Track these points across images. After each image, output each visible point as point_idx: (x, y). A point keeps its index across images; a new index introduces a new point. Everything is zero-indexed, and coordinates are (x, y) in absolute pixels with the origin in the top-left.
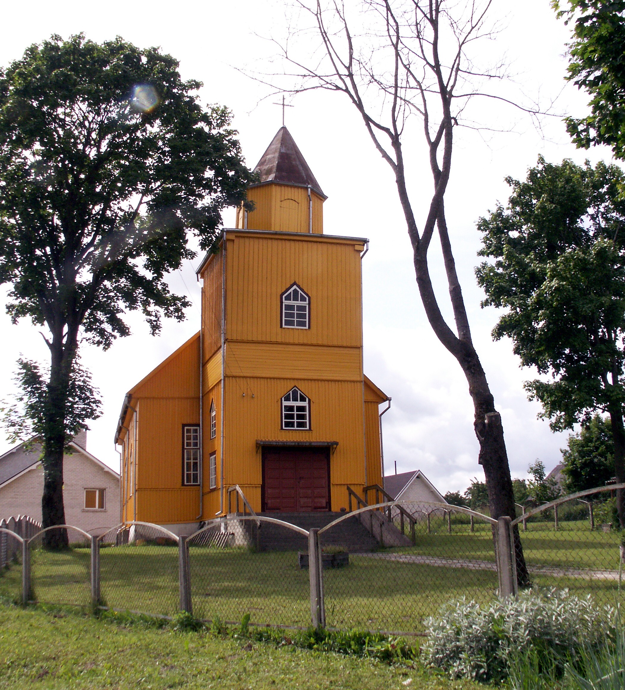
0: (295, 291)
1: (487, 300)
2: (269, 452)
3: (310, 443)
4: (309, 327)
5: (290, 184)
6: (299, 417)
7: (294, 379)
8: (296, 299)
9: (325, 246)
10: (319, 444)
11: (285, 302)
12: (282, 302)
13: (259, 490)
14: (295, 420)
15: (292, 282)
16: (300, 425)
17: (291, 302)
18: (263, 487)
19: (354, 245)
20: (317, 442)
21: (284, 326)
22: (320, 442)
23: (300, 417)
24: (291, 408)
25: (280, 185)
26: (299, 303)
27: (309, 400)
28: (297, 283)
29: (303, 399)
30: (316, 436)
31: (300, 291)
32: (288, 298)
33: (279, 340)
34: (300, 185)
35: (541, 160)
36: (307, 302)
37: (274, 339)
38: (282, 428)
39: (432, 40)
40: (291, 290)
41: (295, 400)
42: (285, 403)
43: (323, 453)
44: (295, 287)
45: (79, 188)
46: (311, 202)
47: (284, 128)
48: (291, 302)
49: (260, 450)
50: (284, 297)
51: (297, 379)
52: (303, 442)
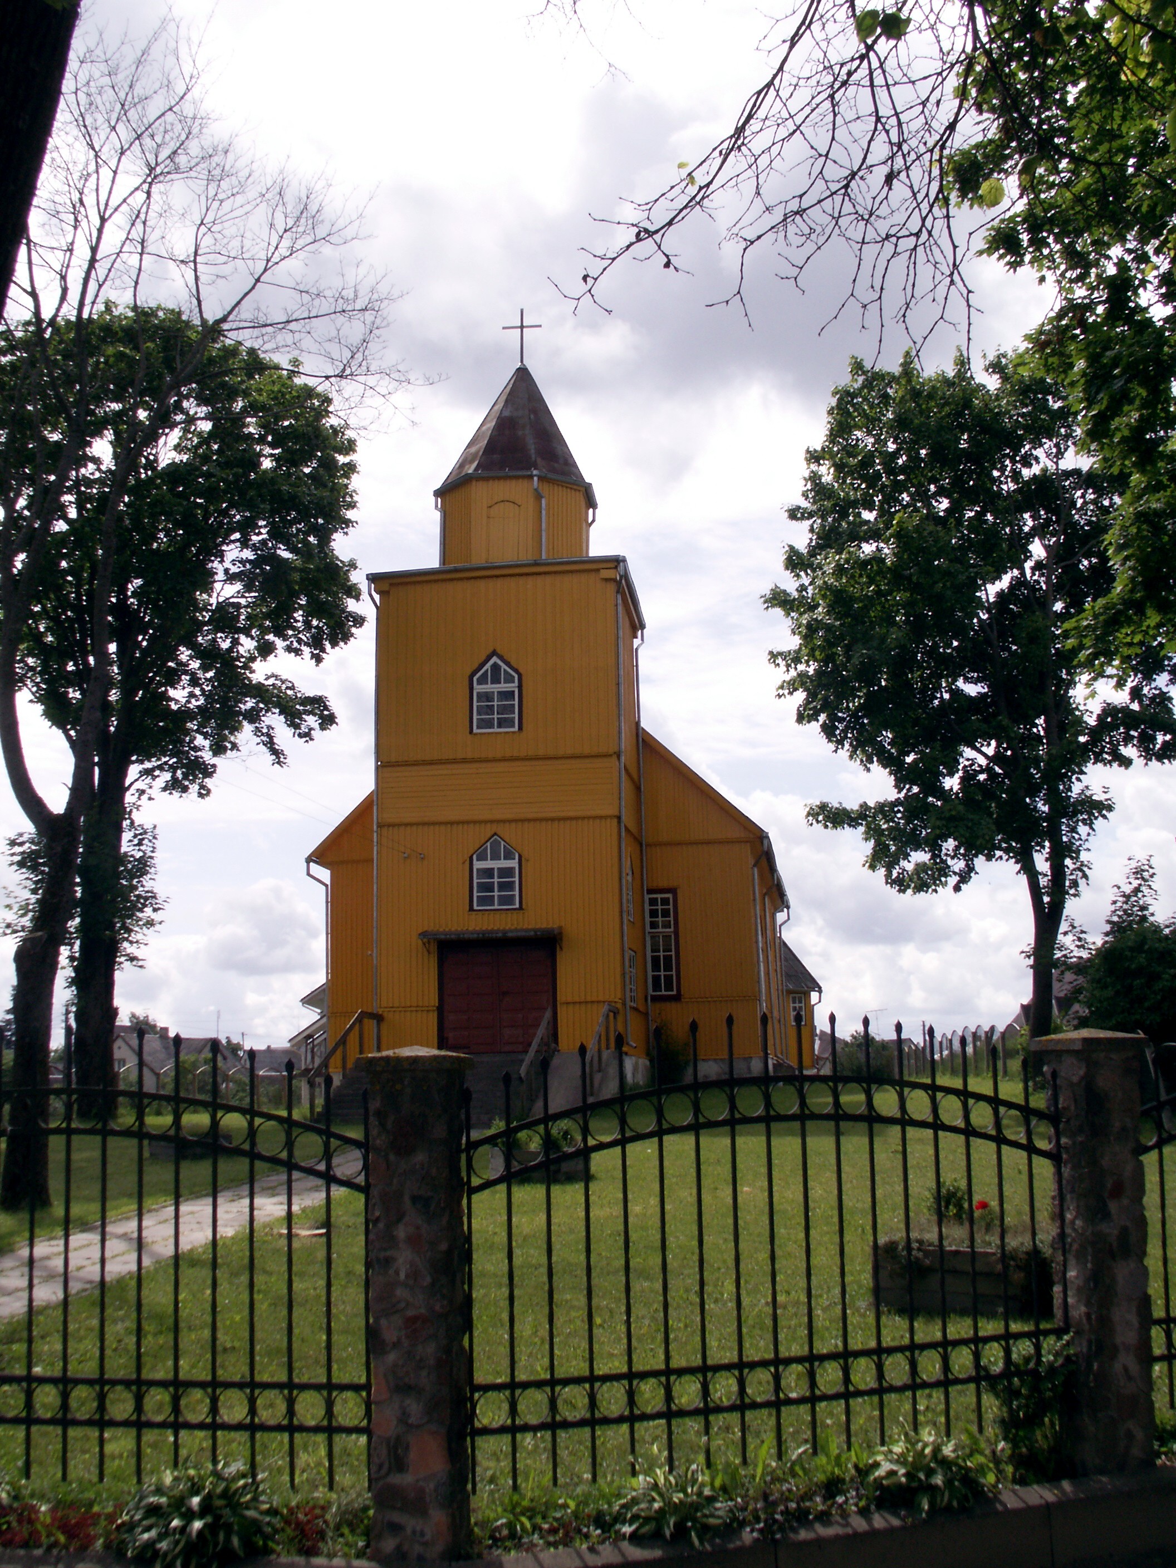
0: (496, 667)
1: (798, 652)
2: (450, 950)
3: (505, 932)
4: (520, 728)
5: (501, 474)
6: (503, 886)
7: (492, 822)
8: (496, 680)
9: (549, 579)
10: (519, 934)
11: (478, 688)
12: (471, 689)
13: (433, 1018)
14: (496, 893)
15: (491, 650)
16: (503, 900)
17: (489, 687)
18: (440, 1010)
19: (598, 570)
20: (516, 930)
21: (475, 730)
22: (522, 930)
23: (503, 886)
24: (489, 872)
25: (486, 479)
26: (504, 687)
27: (520, 857)
28: (499, 651)
29: (508, 856)
30: (534, 919)
31: (503, 666)
32: (482, 680)
33: (469, 755)
34: (520, 473)
35: (858, 367)
36: (516, 684)
37: (460, 755)
38: (471, 909)
39: (34, 267)
40: (488, 666)
41: (495, 857)
42: (478, 865)
43: (547, 944)
44: (494, 659)
45: (151, 544)
46: (543, 501)
47: (523, 375)
48: (489, 687)
49: (434, 948)
50: (475, 679)
51: (498, 821)
52: (492, 931)
